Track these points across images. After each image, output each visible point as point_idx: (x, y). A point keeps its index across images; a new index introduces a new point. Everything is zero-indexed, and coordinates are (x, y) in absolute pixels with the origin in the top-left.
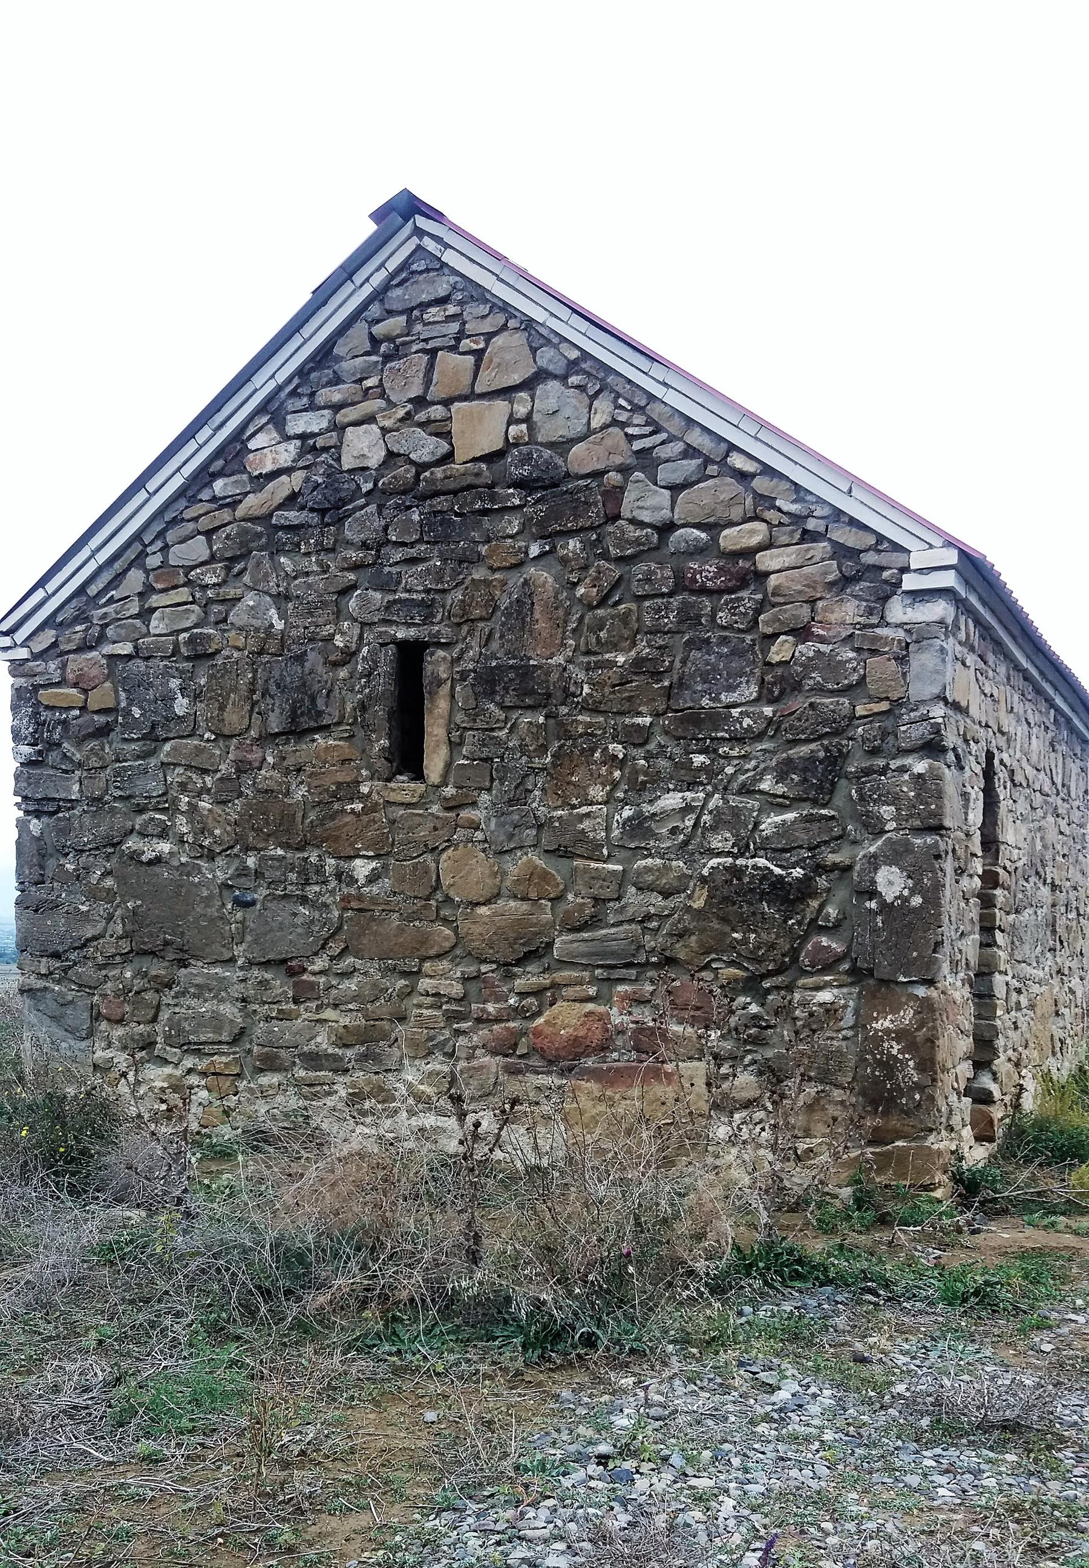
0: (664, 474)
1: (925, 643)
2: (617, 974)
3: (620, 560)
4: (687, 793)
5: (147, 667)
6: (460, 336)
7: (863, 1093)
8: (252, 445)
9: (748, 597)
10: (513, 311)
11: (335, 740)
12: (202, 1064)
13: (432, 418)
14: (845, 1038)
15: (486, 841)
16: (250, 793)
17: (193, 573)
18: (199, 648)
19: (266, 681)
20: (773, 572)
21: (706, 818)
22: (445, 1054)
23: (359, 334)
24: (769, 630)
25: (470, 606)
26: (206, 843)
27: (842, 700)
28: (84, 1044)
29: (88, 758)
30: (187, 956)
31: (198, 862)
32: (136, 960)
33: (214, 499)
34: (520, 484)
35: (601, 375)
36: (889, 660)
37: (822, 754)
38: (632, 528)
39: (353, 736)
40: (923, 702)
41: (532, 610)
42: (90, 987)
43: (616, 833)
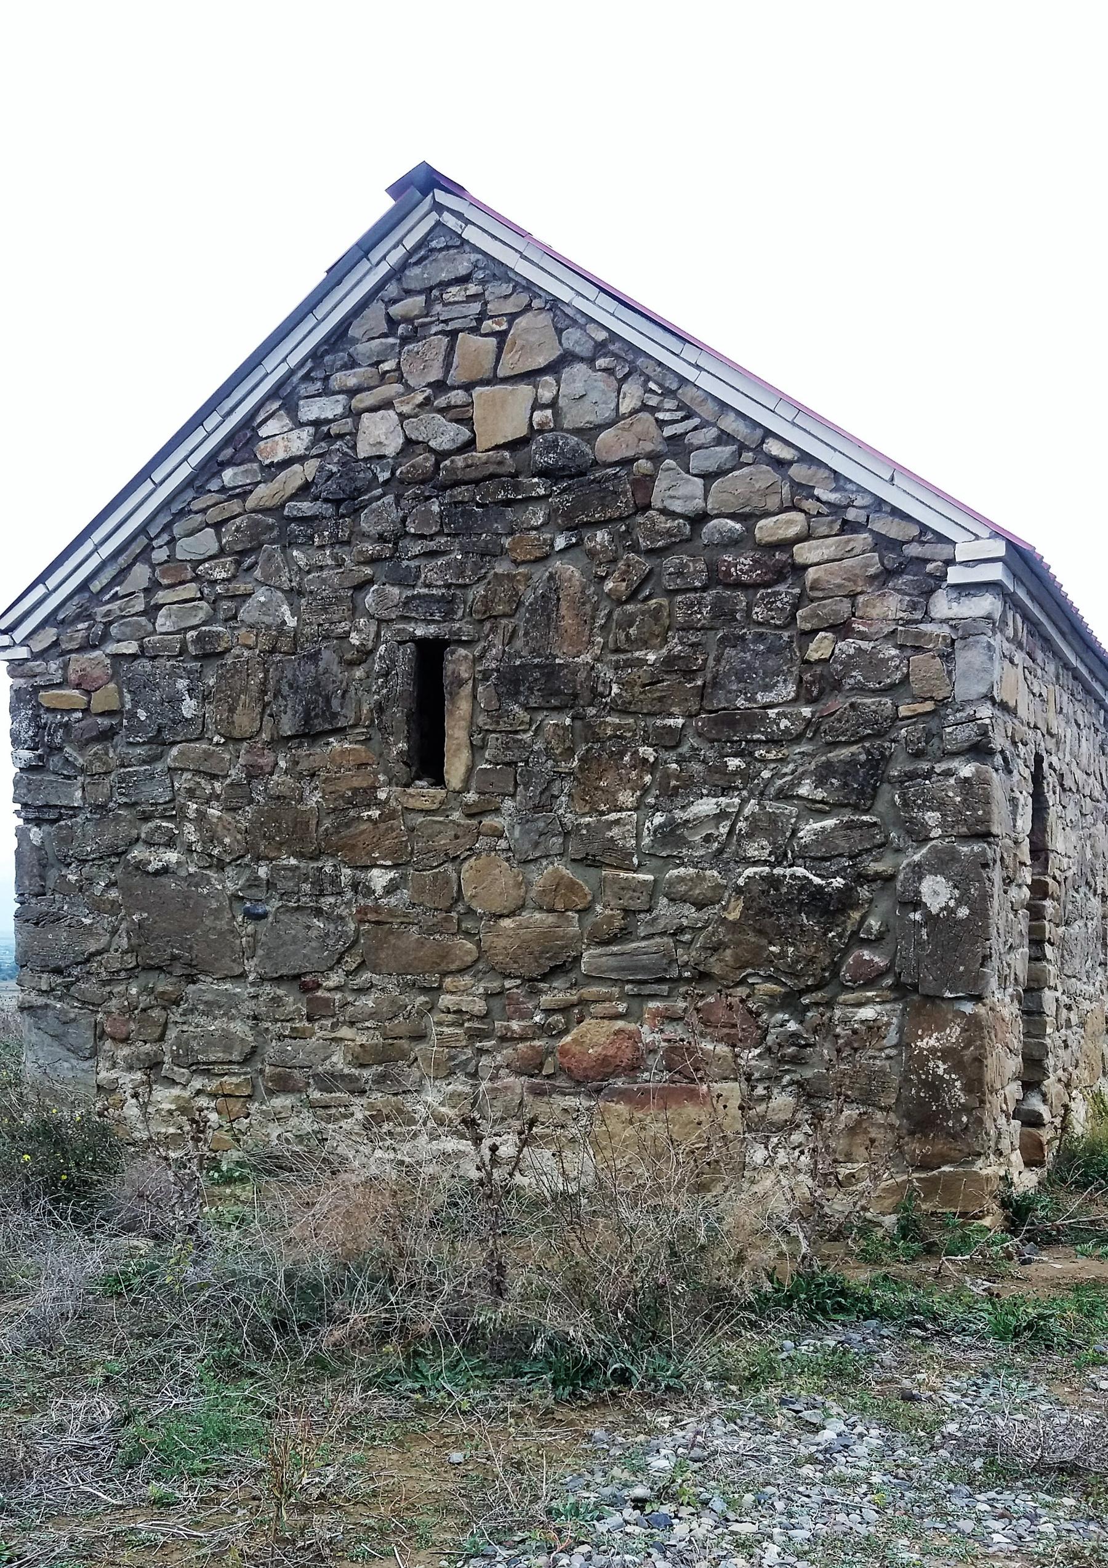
0: (698, 461)
1: (971, 639)
2: (647, 990)
3: (650, 552)
4: (722, 799)
5: (153, 667)
6: (482, 317)
7: (907, 1115)
8: (263, 432)
9: (785, 591)
10: (537, 290)
11: (350, 743)
12: (212, 1085)
13: (452, 403)
14: (888, 1058)
15: (509, 849)
16: (261, 799)
17: (201, 568)
18: (208, 647)
19: (278, 681)
20: (811, 566)
21: (741, 825)
22: (468, 1075)
23: (376, 312)
24: (808, 626)
25: (492, 602)
26: (215, 852)
27: (884, 700)
28: (86, 1065)
29: (91, 763)
30: (196, 971)
31: (208, 872)
32: (143, 977)
33: (223, 489)
34: (544, 473)
35: (630, 357)
36: (934, 657)
37: (863, 757)
38: (663, 518)
39: (370, 739)
40: (970, 702)
41: (557, 605)
42: (93, 1005)
43: (646, 841)
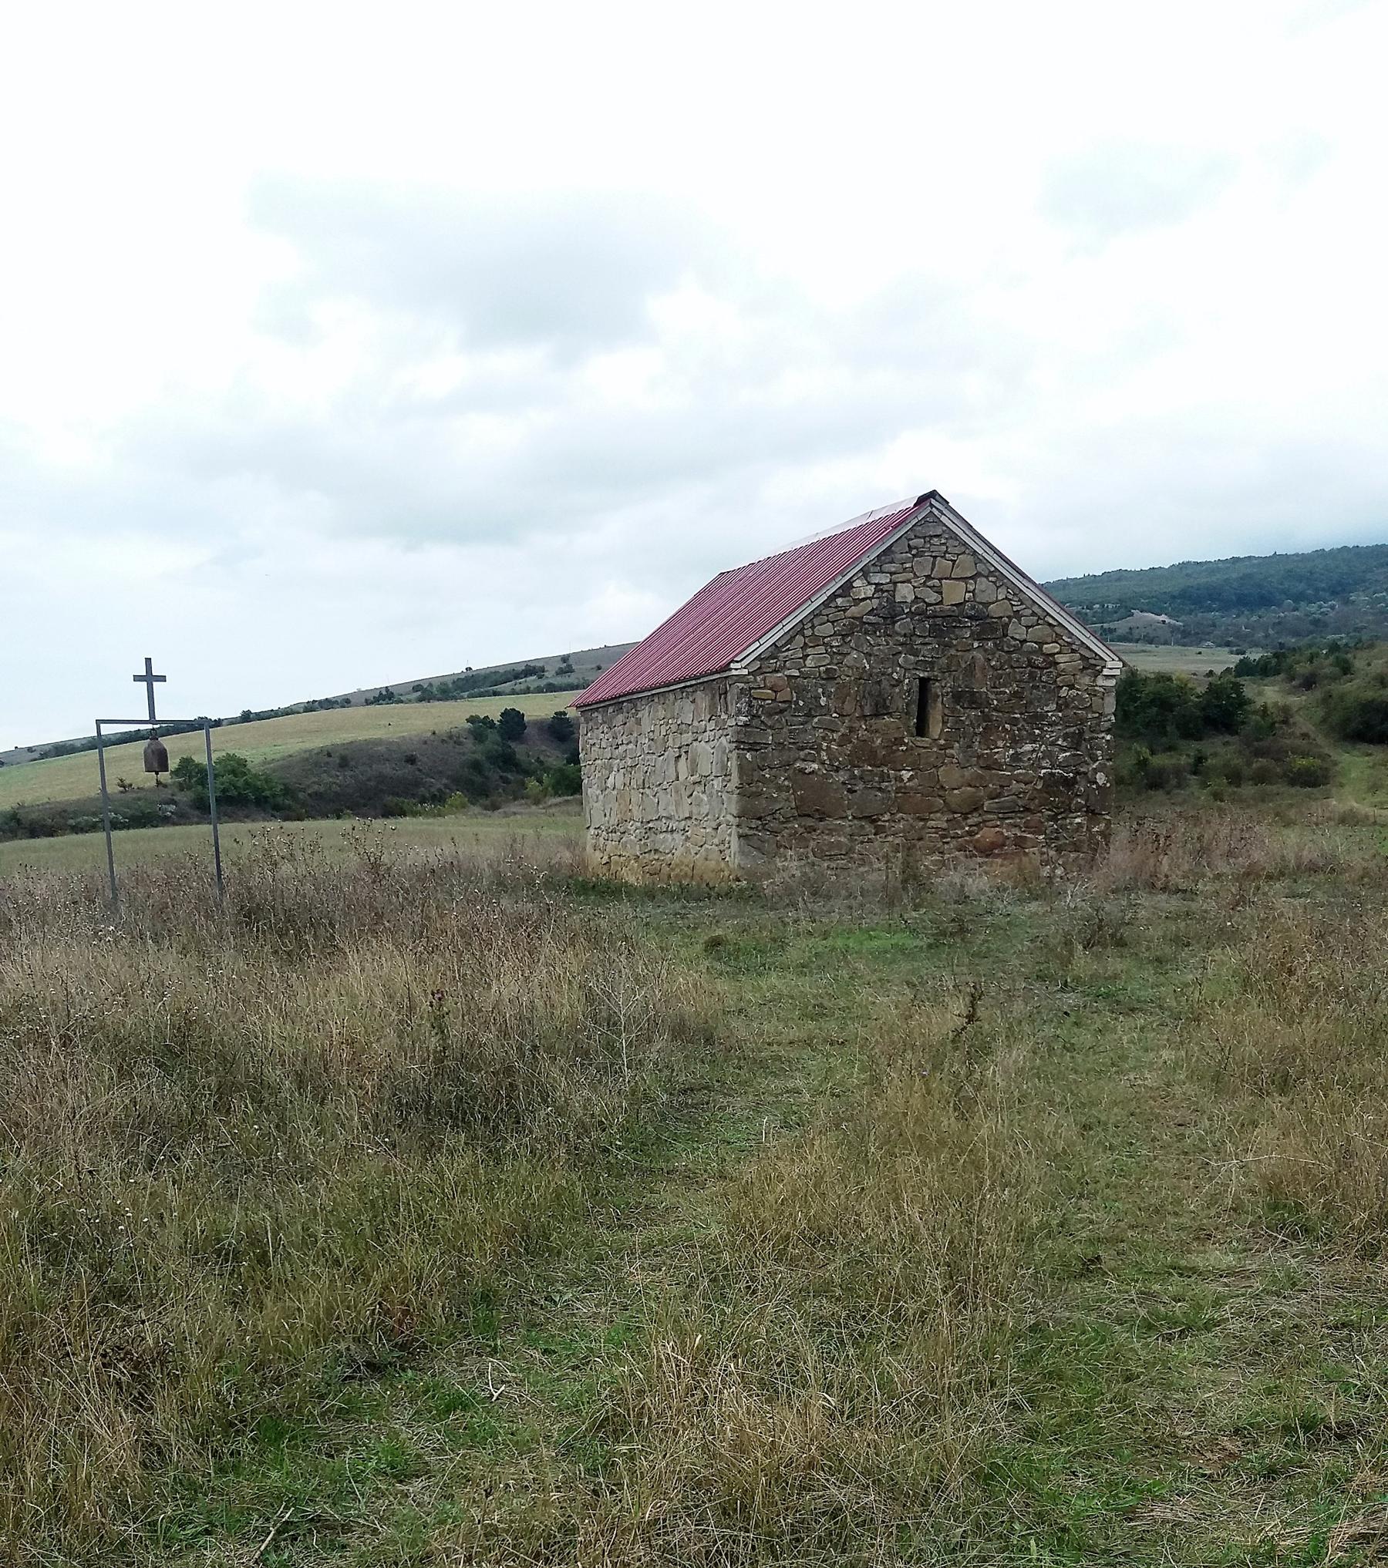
2: (1007, 815)
3: (1007, 652)
6: (946, 552)
8: (854, 585)
33: (836, 607)
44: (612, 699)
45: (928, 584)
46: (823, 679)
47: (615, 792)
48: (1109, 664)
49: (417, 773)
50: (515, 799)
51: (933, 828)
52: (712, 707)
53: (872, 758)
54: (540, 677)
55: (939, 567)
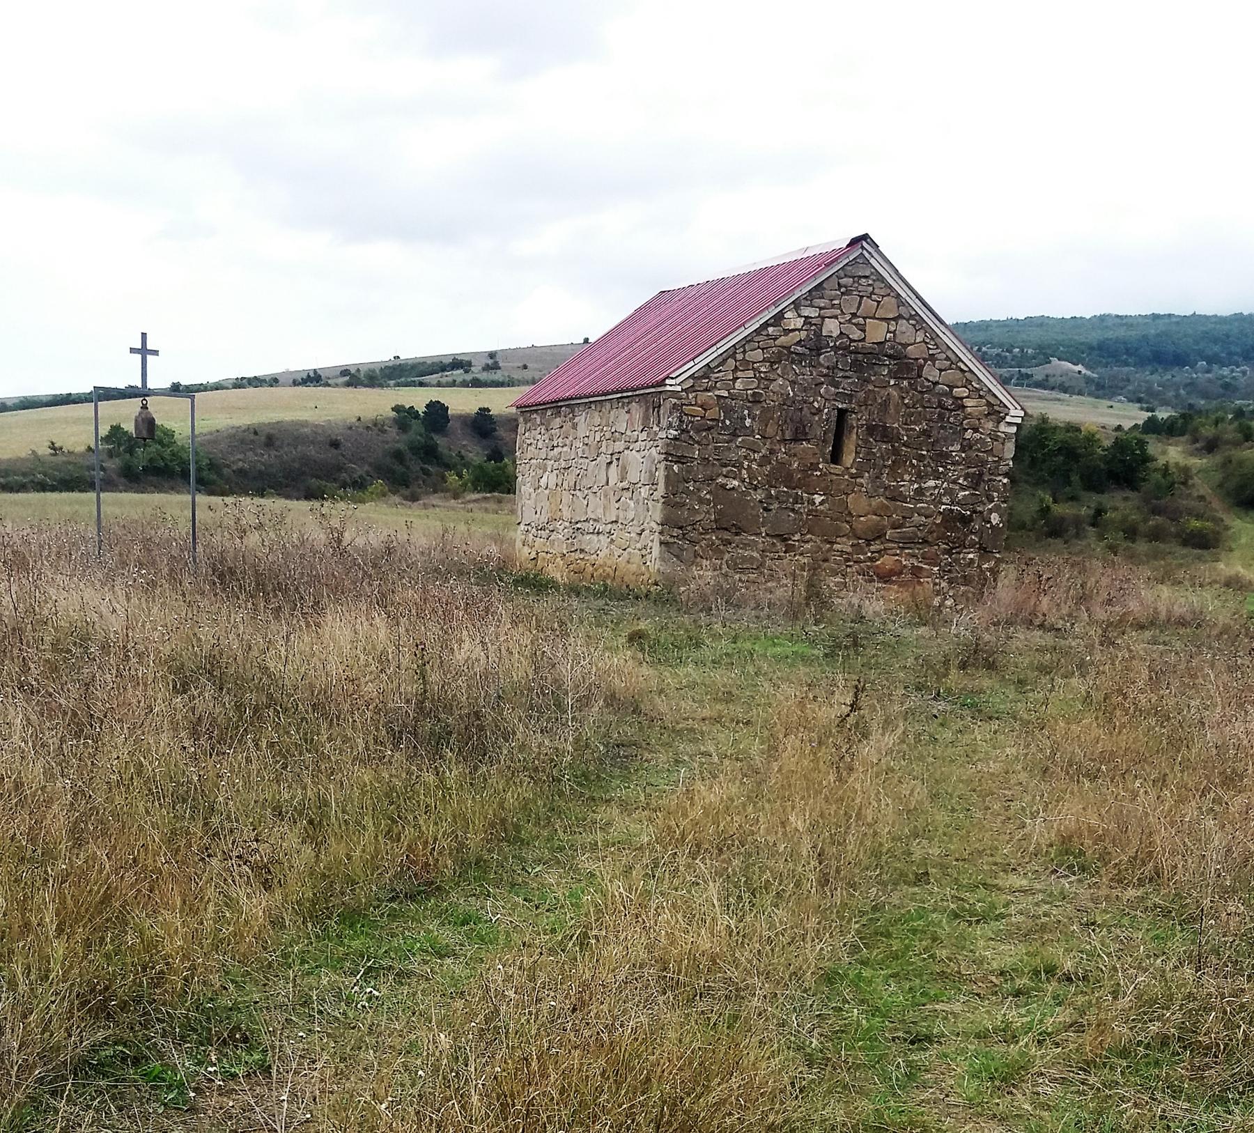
6: (872, 293)
12: (744, 578)
43: (912, 493)
44: (552, 402)
45: (853, 321)
46: (749, 402)
47: (547, 492)
48: (1013, 412)
49: (340, 458)
50: (435, 492)
51: (838, 551)
52: (646, 418)
53: (788, 480)
54: (466, 372)
55: (865, 306)
